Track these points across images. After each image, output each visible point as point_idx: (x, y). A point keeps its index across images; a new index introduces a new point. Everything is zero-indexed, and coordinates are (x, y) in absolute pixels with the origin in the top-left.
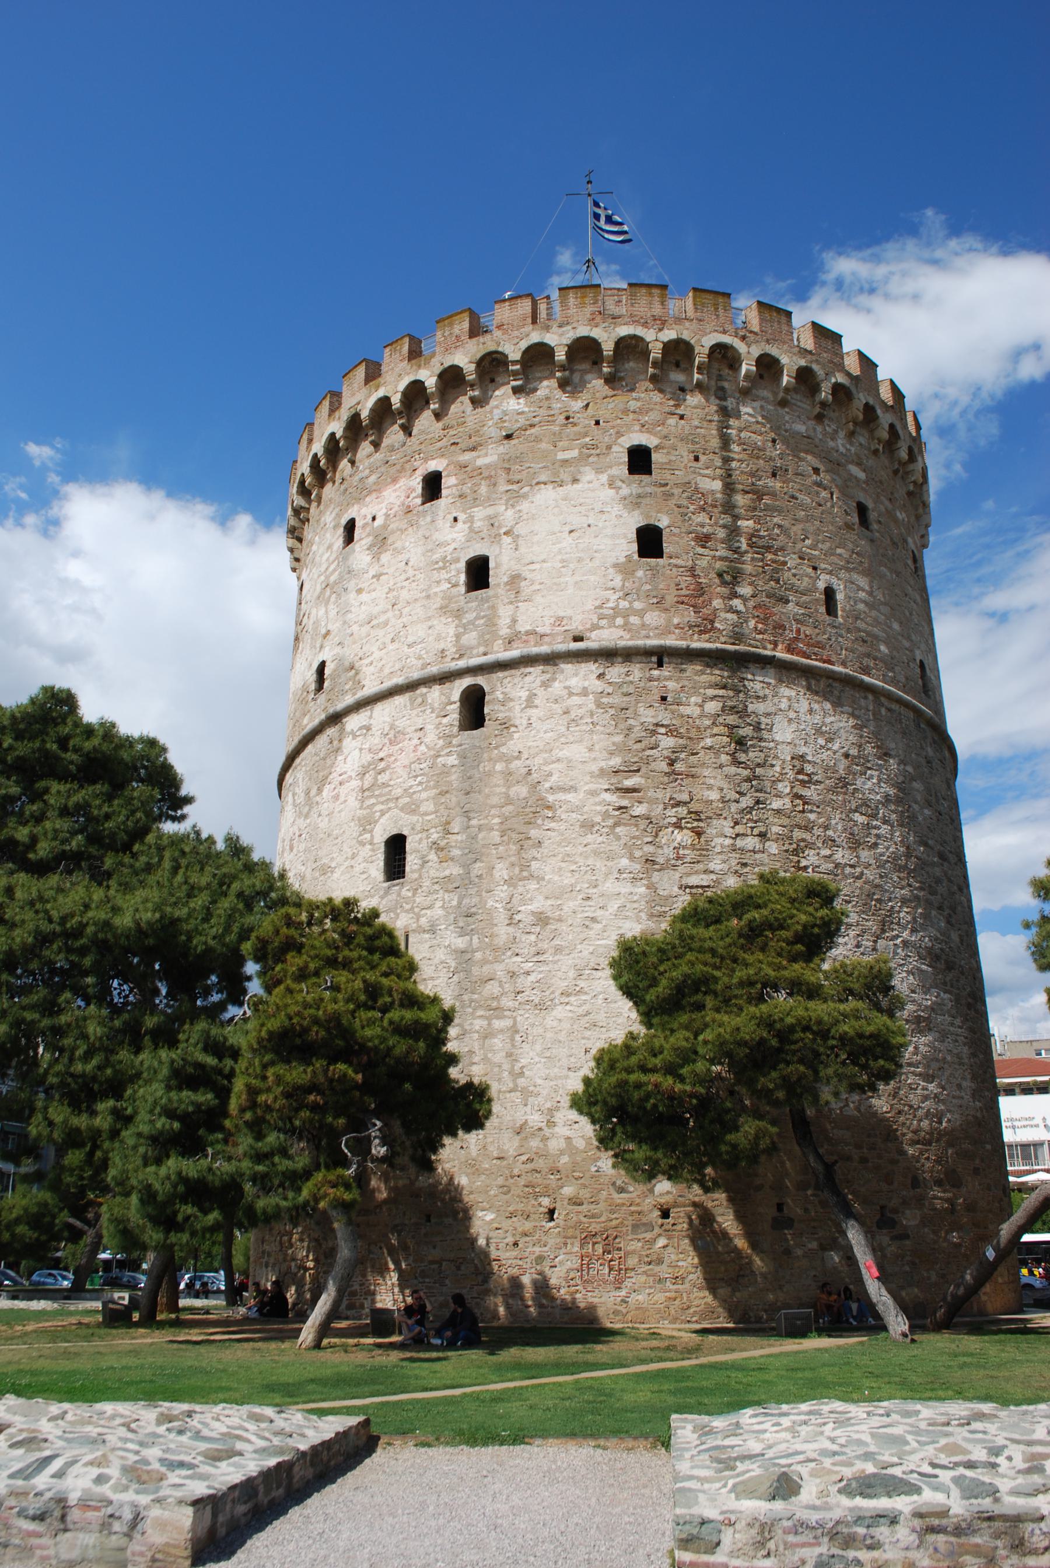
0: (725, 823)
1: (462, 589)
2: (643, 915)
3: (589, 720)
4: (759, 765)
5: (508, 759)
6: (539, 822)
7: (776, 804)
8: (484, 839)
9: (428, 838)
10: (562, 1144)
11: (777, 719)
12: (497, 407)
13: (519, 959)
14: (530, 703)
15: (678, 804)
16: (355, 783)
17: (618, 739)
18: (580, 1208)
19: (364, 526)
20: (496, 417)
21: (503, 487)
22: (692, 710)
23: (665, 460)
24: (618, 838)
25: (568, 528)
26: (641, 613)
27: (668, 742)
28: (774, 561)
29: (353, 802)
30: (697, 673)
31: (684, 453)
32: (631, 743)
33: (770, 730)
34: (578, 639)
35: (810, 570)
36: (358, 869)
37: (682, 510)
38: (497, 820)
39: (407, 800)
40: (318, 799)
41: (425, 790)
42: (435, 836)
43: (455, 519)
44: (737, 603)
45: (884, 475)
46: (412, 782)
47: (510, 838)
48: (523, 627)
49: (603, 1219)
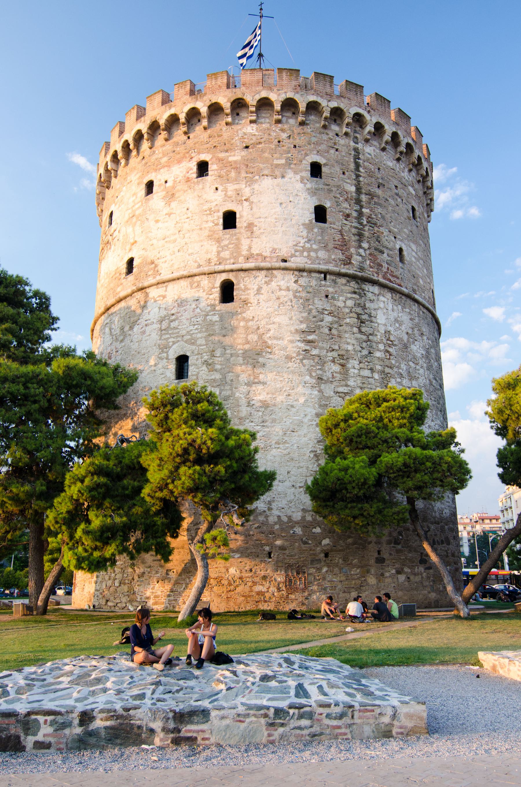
0: (355, 362)
1: (221, 227)
2: (317, 406)
3: (290, 304)
4: (370, 334)
5: (247, 321)
6: (264, 354)
7: (378, 354)
8: (234, 360)
9: (201, 358)
10: (276, 519)
11: (379, 312)
12: (240, 129)
13: (253, 424)
14: (259, 291)
15: (333, 350)
16: (157, 326)
17: (305, 315)
18: (285, 552)
19: (160, 185)
20: (240, 135)
21: (243, 175)
22: (341, 304)
23: (329, 172)
24: (304, 366)
25: (279, 201)
26: (316, 251)
27: (329, 319)
28: (378, 232)
29: (155, 336)
30: (343, 285)
31: (337, 169)
32: (311, 317)
33: (375, 317)
34: (285, 261)
35: (393, 238)
36: (158, 372)
37: (336, 199)
38: (241, 352)
39: (189, 337)
40: (130, 332)
41: (200, 332)
42: (206, 357)
43: (217, 189)
44: (361, 251)
45: (421, 193)
46: (192, 328)
47: (248, 362)
48: (255, 251)
49: (296, 557)
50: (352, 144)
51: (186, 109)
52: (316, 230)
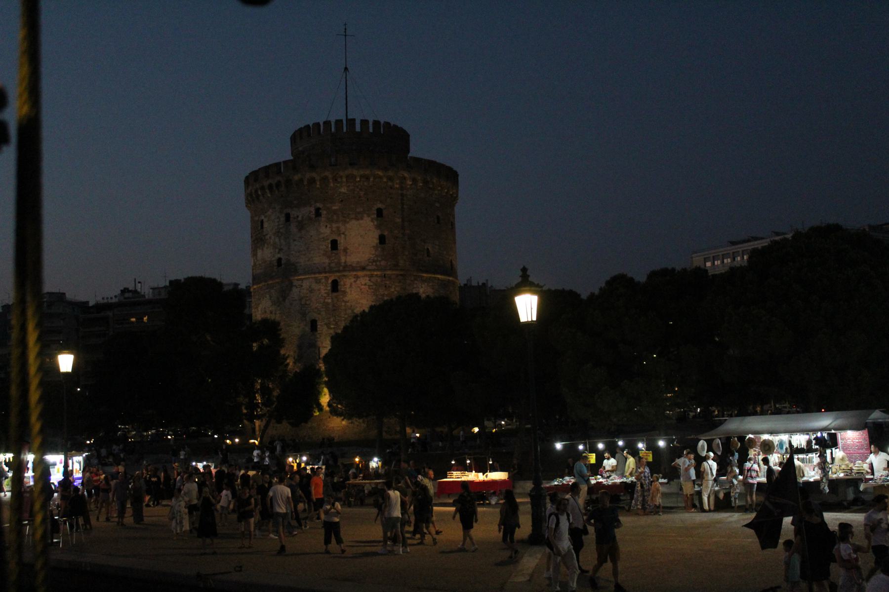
1: (330, 249)
5: (346, 302)
19: (294, 218)
22: (393, 290)
26: (380, 261)
38: (343, 319)
43: (326, 226)
50: (400, 192)
52: (379, 249)
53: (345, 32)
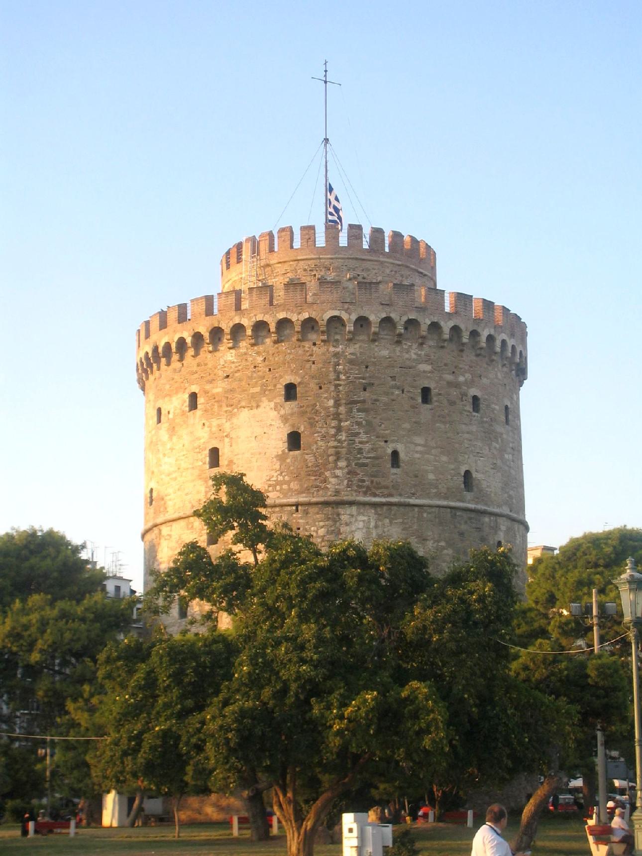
1: (207, 466)
26: (288, 483)
31: (313, 385)
35: (383, 444)
43: (204, 424)
44: (338, 472)
50: (332, 349)
51: (176, 339)
53: (325, 76)
